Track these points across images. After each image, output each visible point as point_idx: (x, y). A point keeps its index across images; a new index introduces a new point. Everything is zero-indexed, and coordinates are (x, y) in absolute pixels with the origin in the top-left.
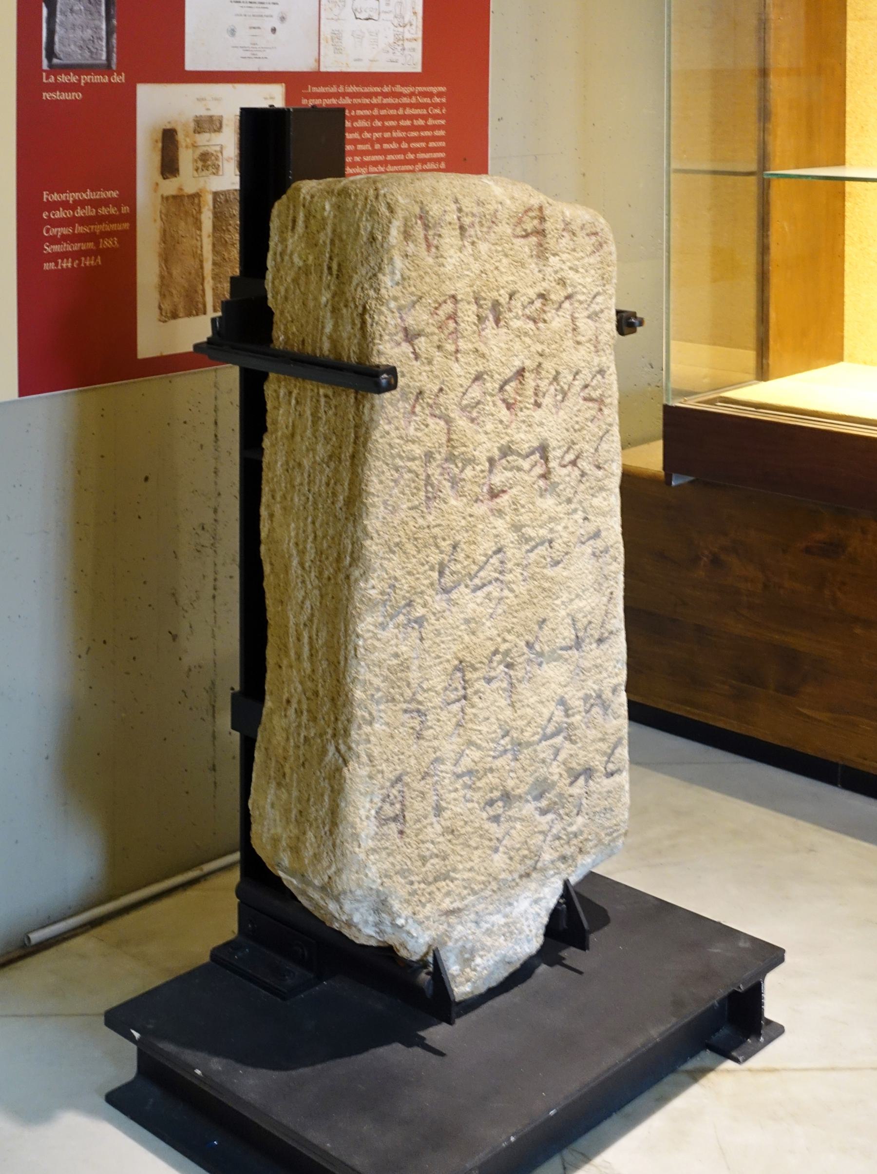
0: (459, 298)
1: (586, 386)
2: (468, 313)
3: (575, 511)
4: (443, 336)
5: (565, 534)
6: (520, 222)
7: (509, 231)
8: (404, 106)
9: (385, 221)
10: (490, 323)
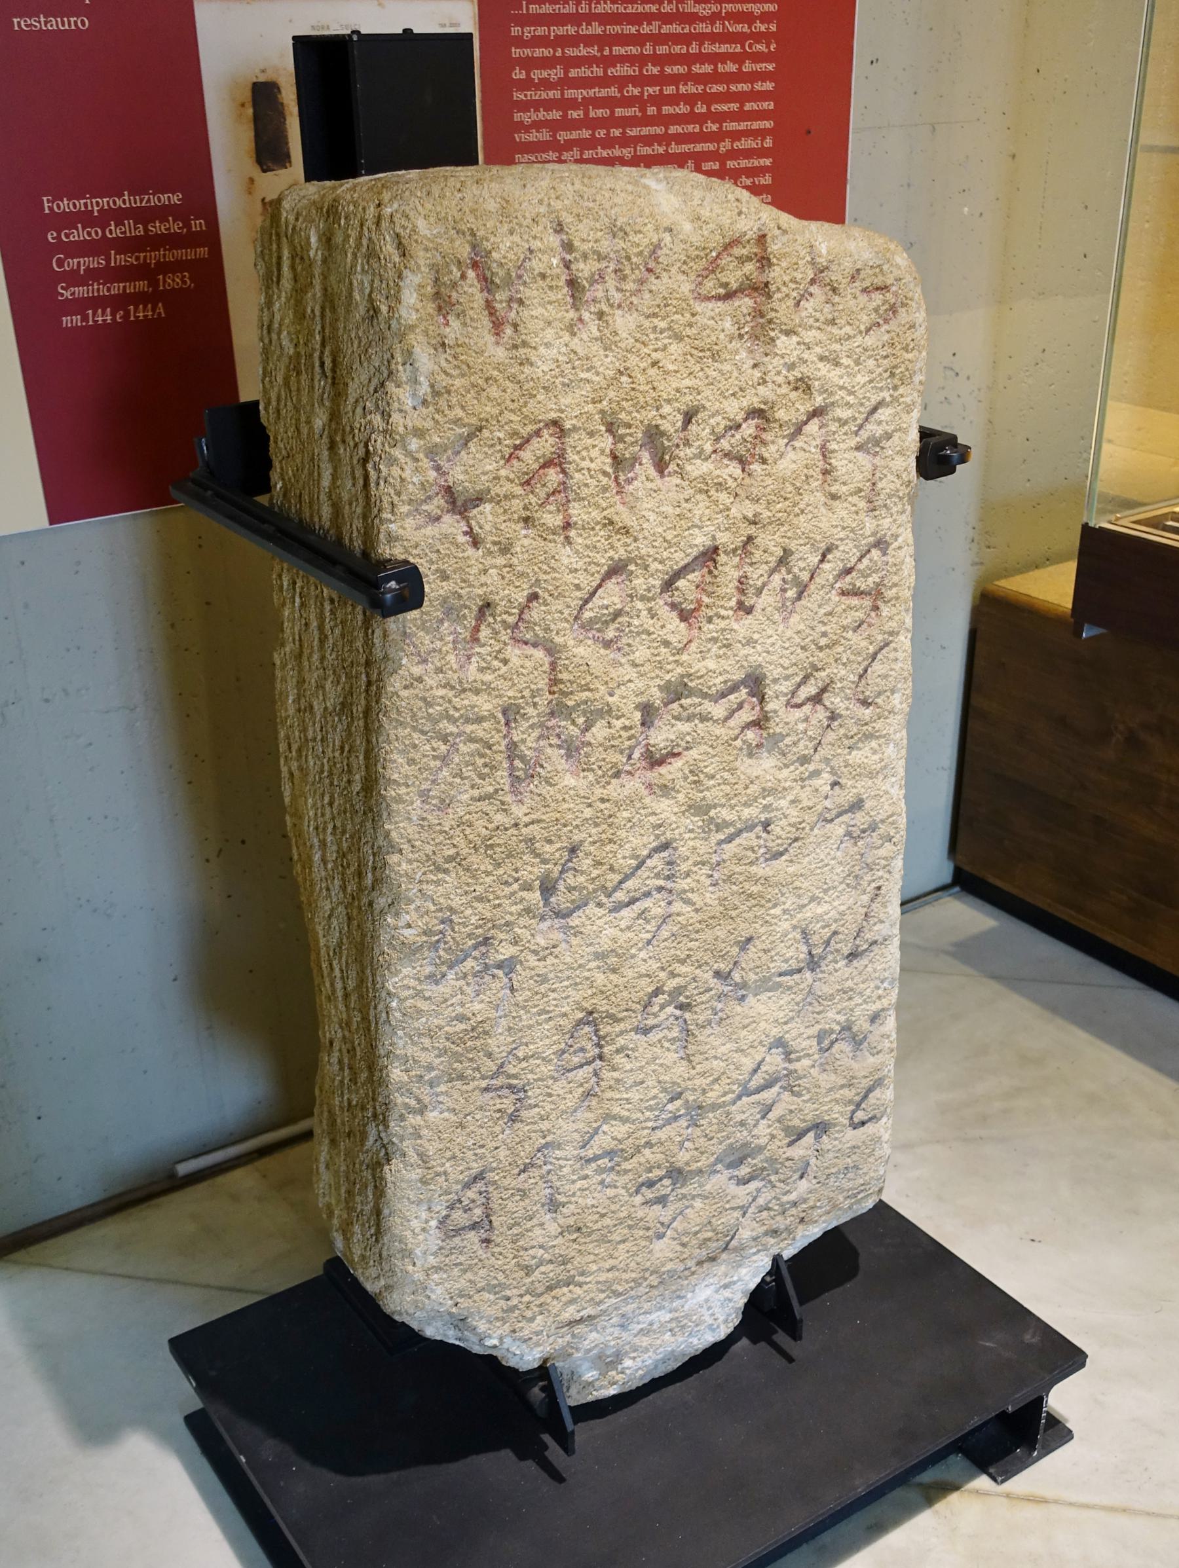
0: (568, 425)
1: (849, 571)
2: (590, 456)
3: (816, 773)
4: (533, 500)
5: (793, 812)
6: (713, 267)
7: (686, 288)
8: (701, 38)
9: (391, 274)
10: (646, 464)
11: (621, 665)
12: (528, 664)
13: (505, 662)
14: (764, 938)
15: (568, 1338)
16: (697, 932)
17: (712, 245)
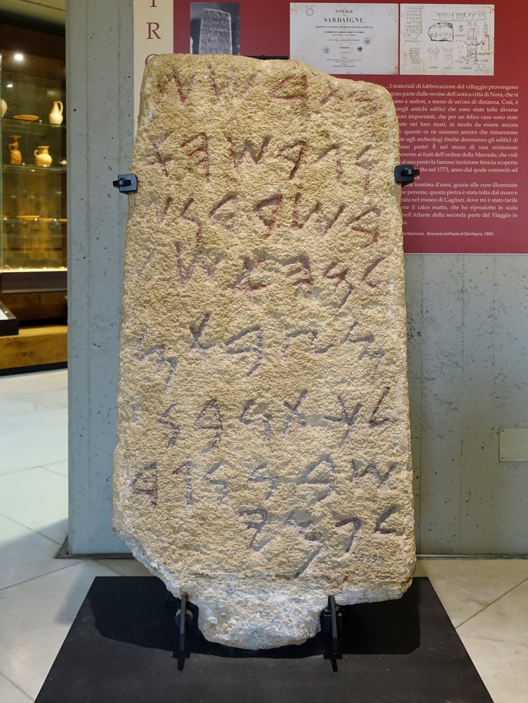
0: (208, 135)
3: (343, 314)
4: (193, 162)
11: (233, 237)
12: (187, 226)
13: (177, 223)
14: (314, 392)
16: (275, 377)
17: (279, 77)
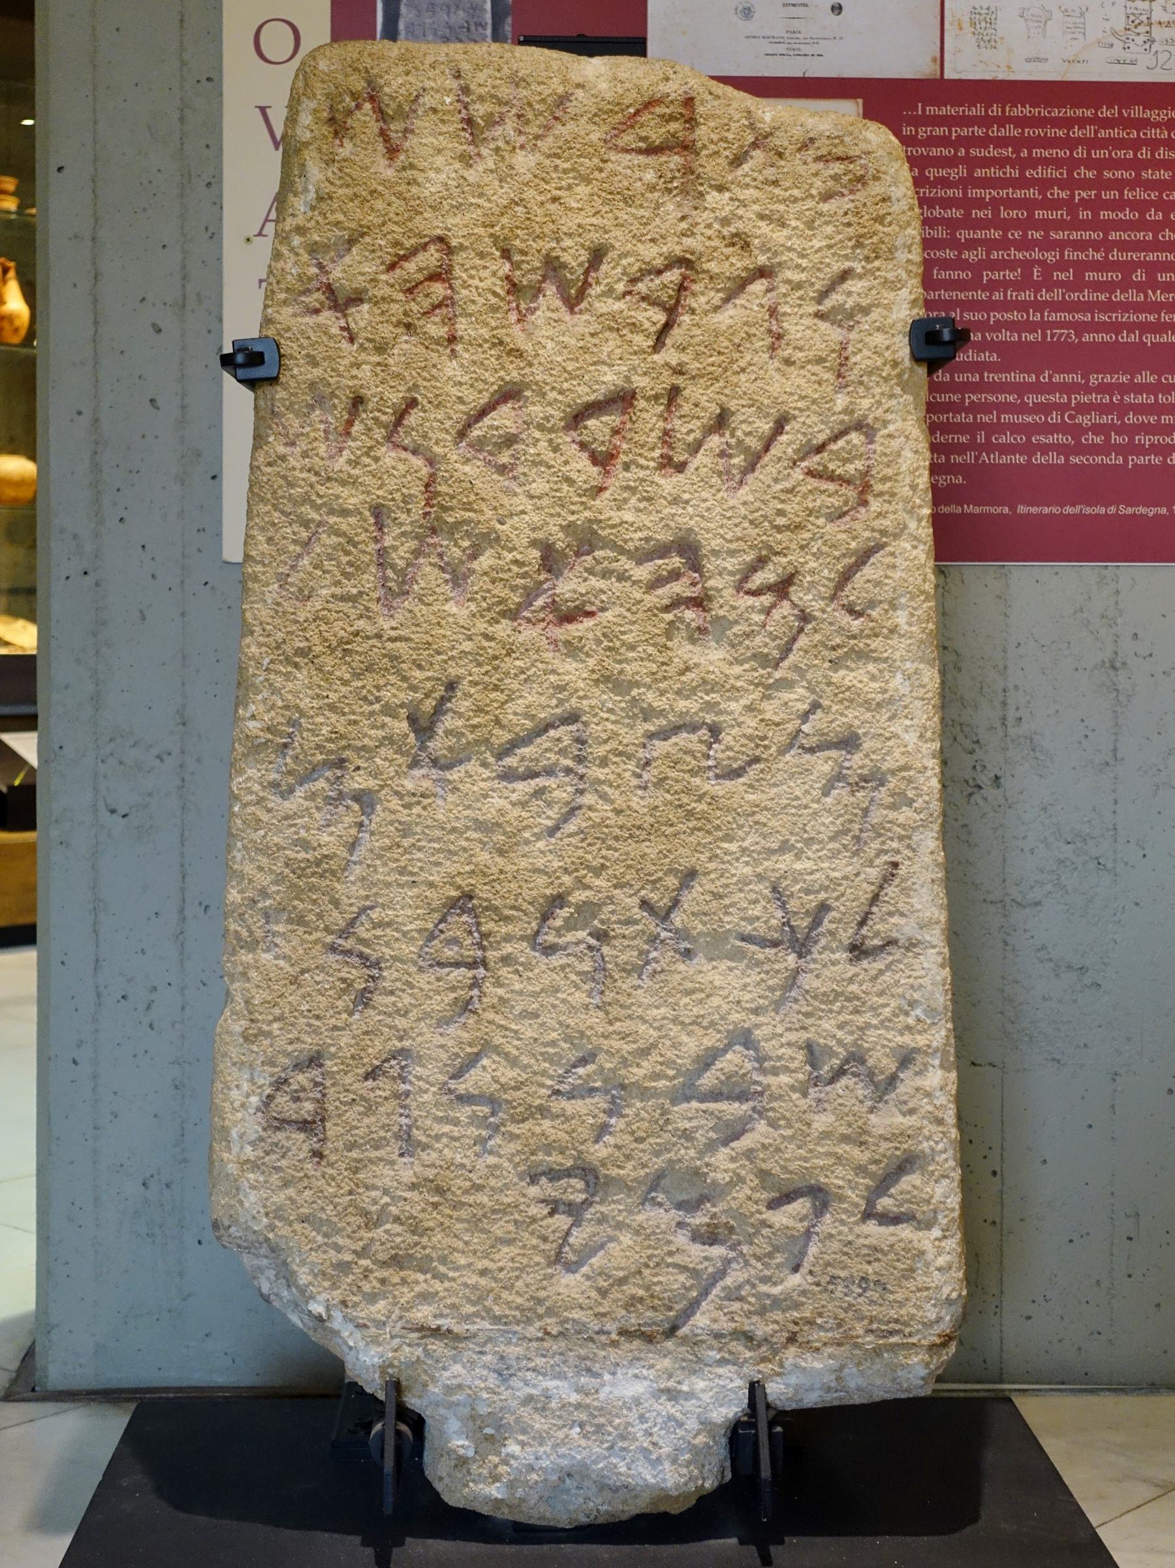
3: (786, 684)
4: (415, 308)
11: (516, 494)
12: (401, 466)
13: (376, 459)
14: (713, 876)
15: (419, 1351)
16: (616, 838)
17: (626, 102)
